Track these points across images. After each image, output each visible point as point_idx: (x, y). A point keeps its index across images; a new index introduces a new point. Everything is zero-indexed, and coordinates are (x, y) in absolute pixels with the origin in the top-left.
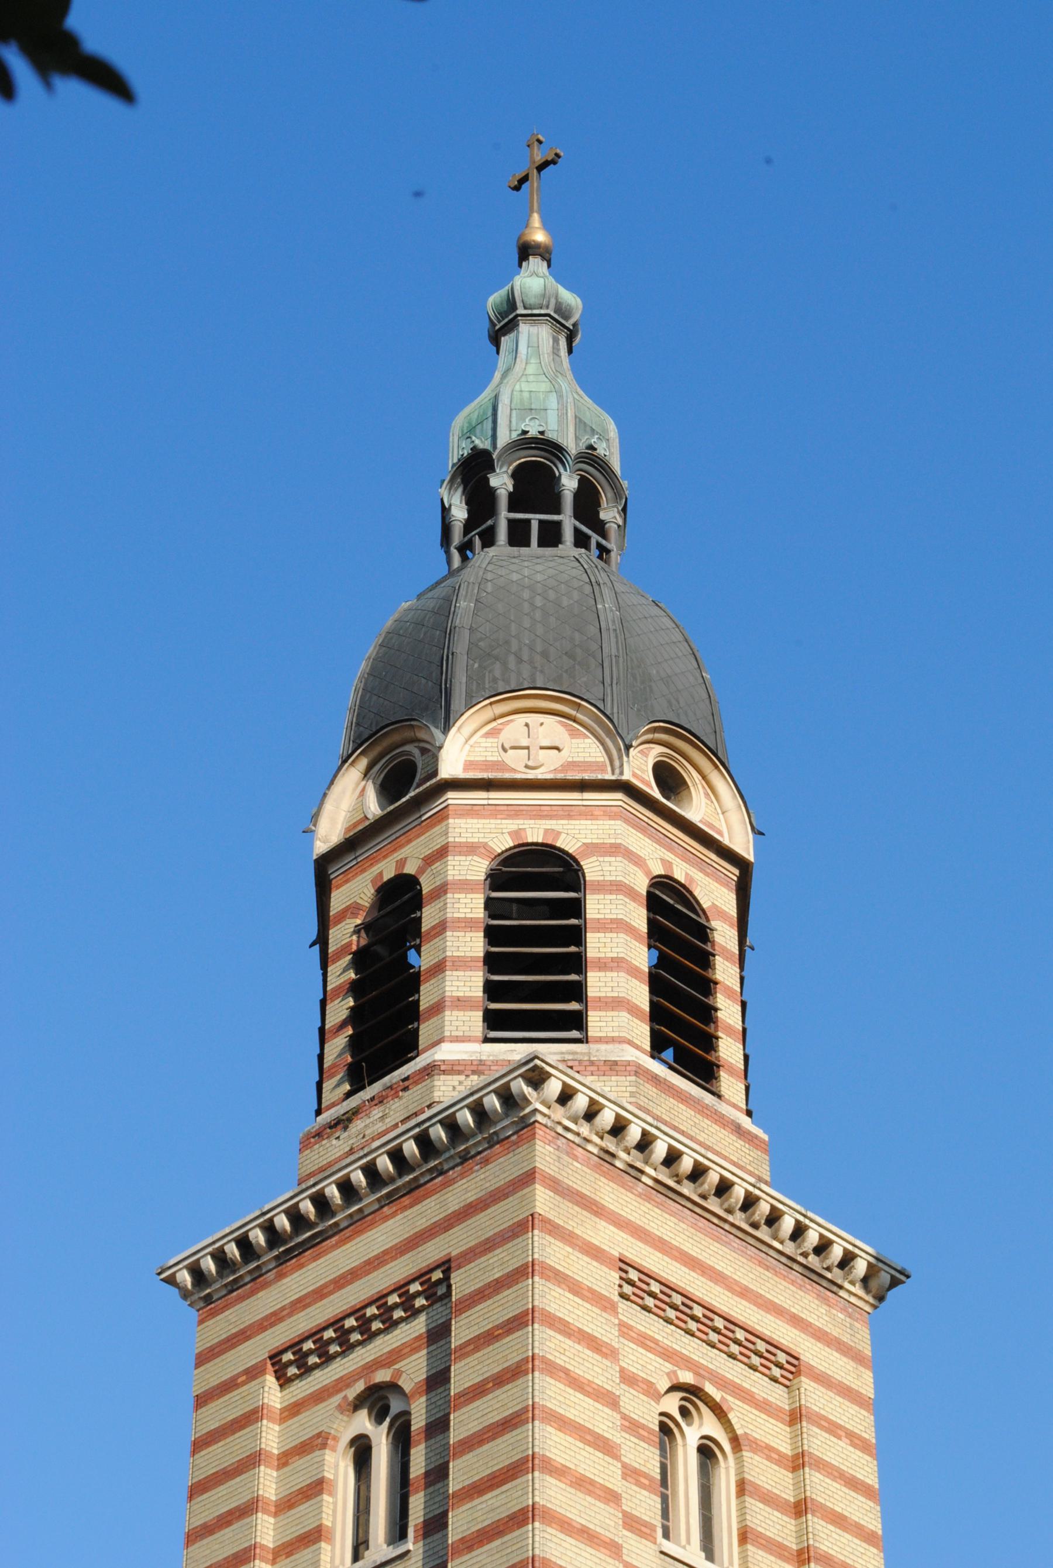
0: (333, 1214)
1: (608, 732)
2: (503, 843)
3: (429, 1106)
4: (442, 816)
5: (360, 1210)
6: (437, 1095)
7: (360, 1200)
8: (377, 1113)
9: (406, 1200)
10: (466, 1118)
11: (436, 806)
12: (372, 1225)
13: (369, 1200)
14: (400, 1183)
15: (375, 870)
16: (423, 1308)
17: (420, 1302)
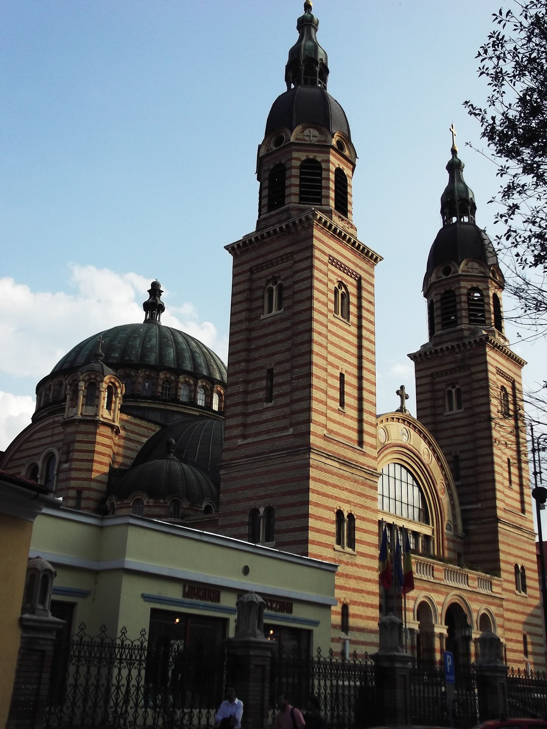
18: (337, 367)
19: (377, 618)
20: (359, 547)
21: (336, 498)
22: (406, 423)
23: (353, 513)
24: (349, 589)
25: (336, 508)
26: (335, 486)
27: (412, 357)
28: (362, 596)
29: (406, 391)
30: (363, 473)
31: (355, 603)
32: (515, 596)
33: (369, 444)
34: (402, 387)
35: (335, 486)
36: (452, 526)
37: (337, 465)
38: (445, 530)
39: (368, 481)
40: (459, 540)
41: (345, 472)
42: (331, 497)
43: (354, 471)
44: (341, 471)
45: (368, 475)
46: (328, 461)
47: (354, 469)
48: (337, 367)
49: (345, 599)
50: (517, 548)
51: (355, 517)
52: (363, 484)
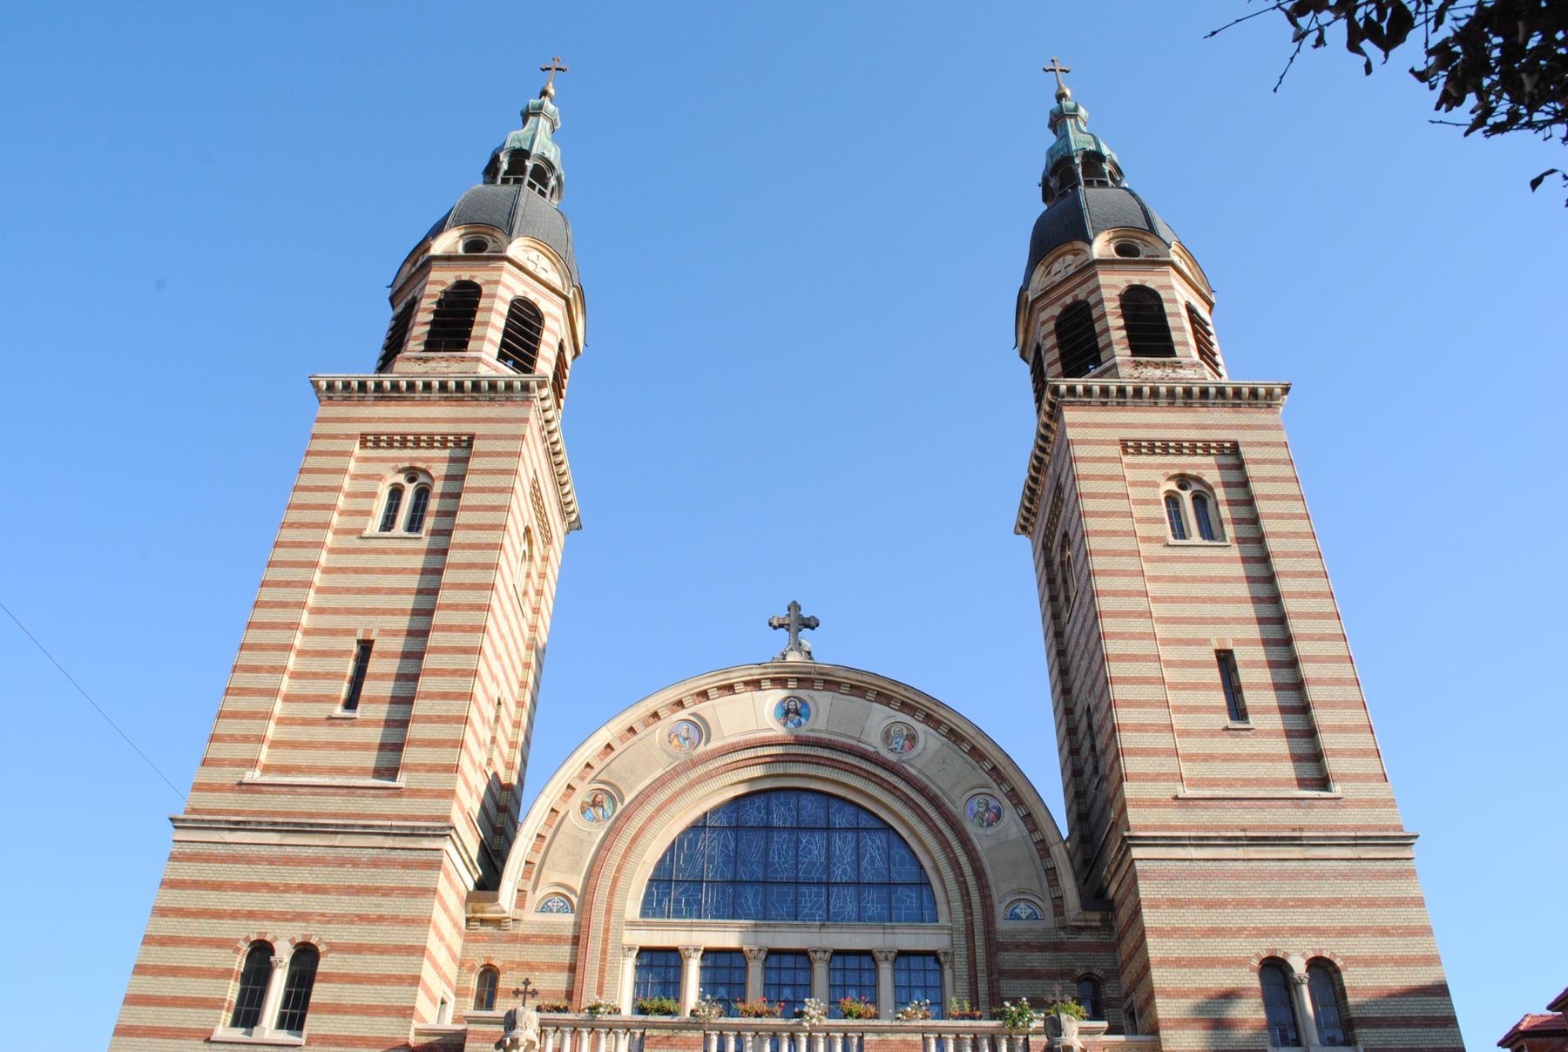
0: (414, 392)
1: (566, 277)
2: (520, 293)
3: (474, 373)
4: (500, 269)
5: (429, 397)
6: (479, 370)
7: (431, 393)
8: (444, 364)
9: (454, 403)
10: (485, 384)
11: (499, 264)
12: (433, 405)
13: (435, 395)
14: (455, 395)
15: (458, 273)
16: (451, 447)
17: (449, 444)
18: (350, 632)
20: (313, 1023)
21: (251, 915)
22: (792, 684)
23: (314, 941)
26: (250, 887)
27: (1020, 530)
29: (805, 613)
30: (380, 838)
33: (425, 765)
34: (795, 607)
35: (250, 887)
36: (1047, 906)
38: (1003, 924)
39: (400, 852)
40: (1085, 938)
42: (234, 915)
43: (338, 840)
47: (339, 836)
48: (350, 632)
50: (1269, 904)
51: (322, 948)
52: (375, 864)
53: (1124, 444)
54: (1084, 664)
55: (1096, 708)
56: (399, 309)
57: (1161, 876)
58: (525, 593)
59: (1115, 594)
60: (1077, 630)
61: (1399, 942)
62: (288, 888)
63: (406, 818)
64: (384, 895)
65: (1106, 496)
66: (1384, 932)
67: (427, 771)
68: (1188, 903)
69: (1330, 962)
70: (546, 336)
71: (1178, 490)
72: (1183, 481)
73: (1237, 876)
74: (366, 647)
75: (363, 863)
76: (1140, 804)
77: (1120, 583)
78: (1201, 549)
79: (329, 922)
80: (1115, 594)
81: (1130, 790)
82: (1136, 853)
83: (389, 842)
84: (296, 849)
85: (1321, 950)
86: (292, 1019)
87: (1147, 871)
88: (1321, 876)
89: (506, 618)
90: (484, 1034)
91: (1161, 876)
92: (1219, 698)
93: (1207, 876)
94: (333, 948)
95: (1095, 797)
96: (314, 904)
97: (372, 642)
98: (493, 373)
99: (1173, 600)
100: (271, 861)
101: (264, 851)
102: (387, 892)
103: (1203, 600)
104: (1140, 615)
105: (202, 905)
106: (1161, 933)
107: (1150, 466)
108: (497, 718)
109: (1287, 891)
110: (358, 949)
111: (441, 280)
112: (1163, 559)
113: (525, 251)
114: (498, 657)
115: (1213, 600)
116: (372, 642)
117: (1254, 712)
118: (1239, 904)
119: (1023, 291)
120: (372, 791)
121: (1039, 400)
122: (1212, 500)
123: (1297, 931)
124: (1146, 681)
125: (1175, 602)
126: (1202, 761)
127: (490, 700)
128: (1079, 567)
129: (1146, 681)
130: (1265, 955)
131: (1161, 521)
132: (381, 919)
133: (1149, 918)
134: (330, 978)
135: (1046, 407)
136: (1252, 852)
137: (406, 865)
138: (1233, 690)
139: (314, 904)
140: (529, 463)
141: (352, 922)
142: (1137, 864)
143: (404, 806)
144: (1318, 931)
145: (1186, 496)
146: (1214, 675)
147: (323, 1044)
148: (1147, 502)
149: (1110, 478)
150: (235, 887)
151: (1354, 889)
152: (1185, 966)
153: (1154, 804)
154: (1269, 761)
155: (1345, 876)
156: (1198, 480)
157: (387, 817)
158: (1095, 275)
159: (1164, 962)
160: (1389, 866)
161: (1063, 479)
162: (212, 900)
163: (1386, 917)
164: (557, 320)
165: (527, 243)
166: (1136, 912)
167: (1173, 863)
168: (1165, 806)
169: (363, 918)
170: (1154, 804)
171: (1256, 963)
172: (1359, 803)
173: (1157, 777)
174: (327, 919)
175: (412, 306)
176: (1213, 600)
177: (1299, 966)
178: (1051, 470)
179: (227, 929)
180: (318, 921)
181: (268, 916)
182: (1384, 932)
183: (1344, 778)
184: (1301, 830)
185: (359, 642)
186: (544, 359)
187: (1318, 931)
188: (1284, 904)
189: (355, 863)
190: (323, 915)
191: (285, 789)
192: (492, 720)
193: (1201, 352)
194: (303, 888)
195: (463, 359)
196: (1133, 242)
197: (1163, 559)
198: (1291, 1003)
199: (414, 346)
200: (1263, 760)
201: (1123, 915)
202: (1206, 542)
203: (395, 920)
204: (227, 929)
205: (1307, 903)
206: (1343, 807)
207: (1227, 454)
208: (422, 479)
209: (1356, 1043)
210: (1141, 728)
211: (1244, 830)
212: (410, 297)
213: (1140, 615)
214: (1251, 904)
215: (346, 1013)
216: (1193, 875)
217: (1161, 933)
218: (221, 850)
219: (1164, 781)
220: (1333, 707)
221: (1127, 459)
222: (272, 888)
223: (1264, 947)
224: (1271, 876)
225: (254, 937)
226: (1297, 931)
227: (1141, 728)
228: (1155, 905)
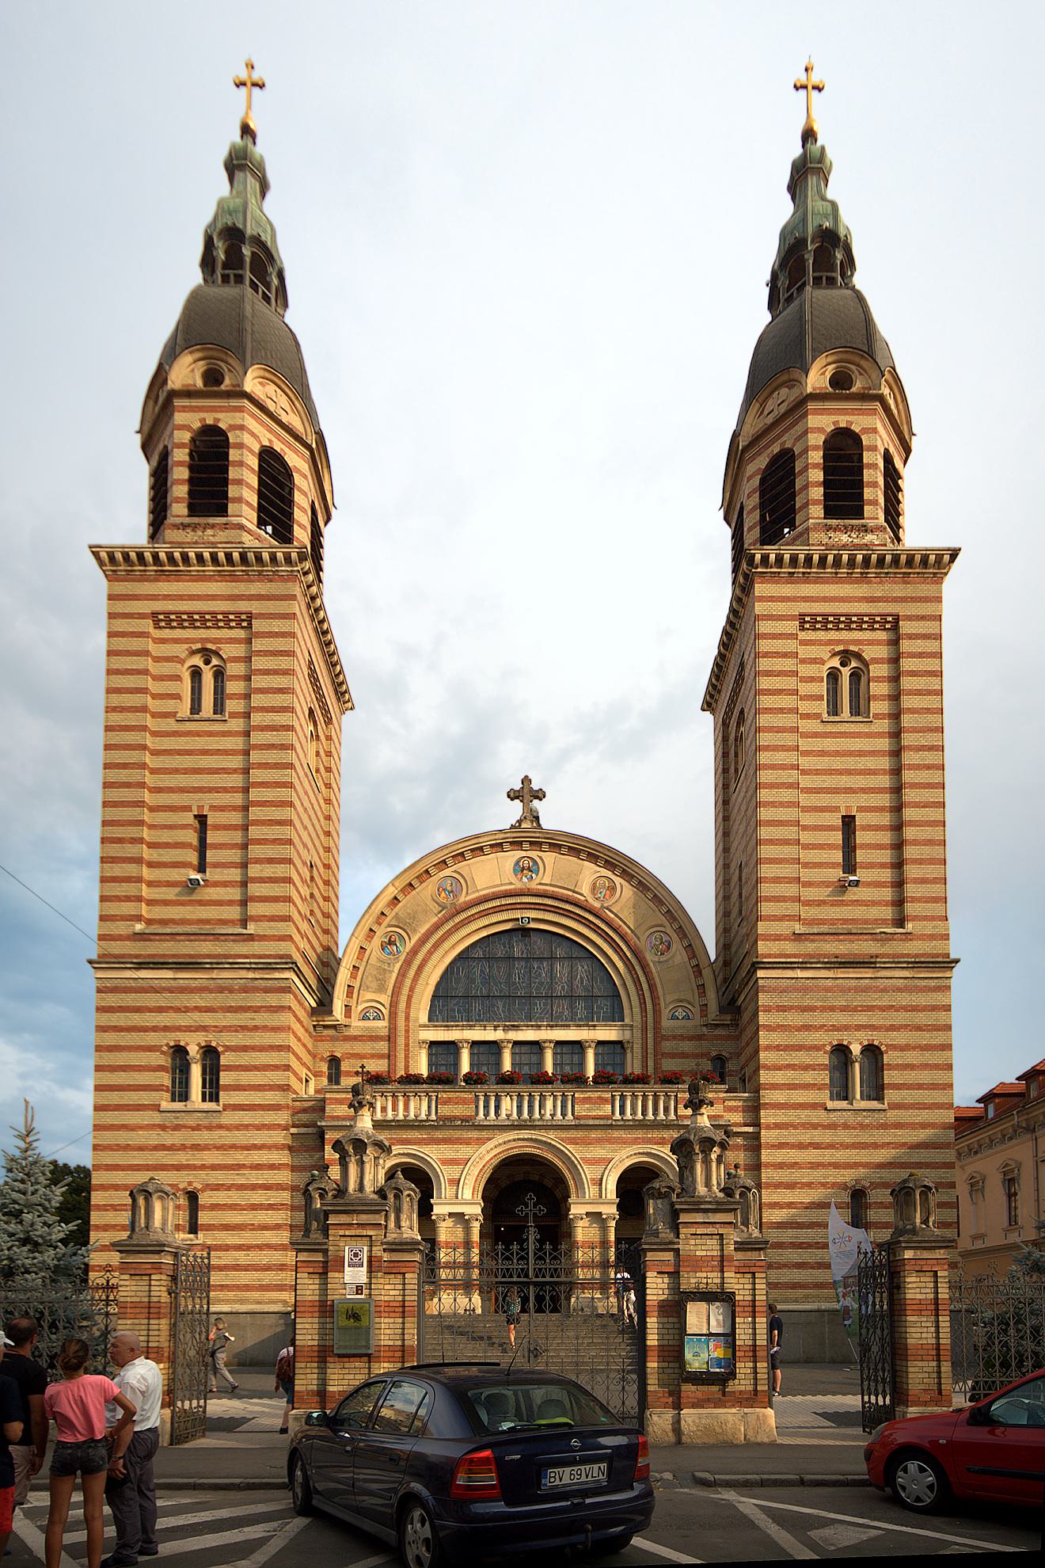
18: (188, 809)
19: (284, 1204)
21: (166, 1029)
23: (214, 1044)
24: (203, 1167)
25: (167, 1045)
26: (160, 1010)
28: (238, 1174)
30: (244, 972)
31: (209, 1187)
32: (822, 1113)
33: (266, 916)
37: (169, 974)
41: (191, 982)
42: (155, 1029)
44: (181, 981)
45: (261, 971)
46: (143, 974)
47: (216, 971)
48: (188, 809)
49: (190, 1183)
50: (844, 1009)
51: (220, 1049)
52: (245, 990)
53: (801, 617)
54: (741, 830)
55: (746, 865)
56: (155, 462)
57: (775, 990)
58: (317, 771)
59: (773, 767)
60: (740, 800)
61: (927, 1035)
62: (187, 1010)
63: (260, 957)
64: (255, 1012)
65: (780, 673)
66: (919, 1028)
67: (268, 921)
68: (790, 1008)
69: (877, 1047)
70: (298, 497)
71: (839, 667)
72: (846, 656)
73: (827, 990)
74: (202, 819)
75: (236, 990)
76: (768, 938)
77: (780, 757)
78: (847, 725)
79: (221, 1032)
80: (773, 767)
81: (762, 928)
82: (760, 974)
83: (251, 975)
84: (187, 982)
85: (873, 1040)
86: (212, 1091)
87: (765, 986)
88: (884, 990)
89: (306, 793)
90: (336, 1099)
91: (775, 990)
92: (838, 856)
93: (806, 990)
94: (228, 1048)
95: (737, 932)
96: (207, 1019)
97: (206, 816)
98: (257, 544)
99: (817, 772)
100: (171, 990)
101: (164, 984)
102: (256, 1010)
103: (840, 772)
104: (790, 786)
105: (130, 1023)
106: (770, 1028)
107: (819, 643)
108: (312, 878)
109: (859, 1000)
110: (245, 1049)
111: (187, 420)
112: (816, 735)
113: (261, 383)
114: (305, 828)
115: (848, 772)
116: (206, 816)
117: (860, 868)
118: (824, 1009)
119: (735, 436)
120: (231, 937)
121: (735, 570)
122: (866, 676)
123: (859, 1028)
124: (786, 842)
125: (819, 774)
126: (817, 905)
127: (304, 863)
128: (748, 742)
129: (786, 842)
130: (835, 1043)
131: (820, 698)
132: (256, 1028)
133: (763, 1018)
134: (229, 1068)
135: (741, 579)
136: (840, 973)
137: (267, 990)
138: (849, 848)
139: (207, 1019)
140: (302, 643)
141: (237, 1031)
142: (760, 982)
143: (256, 948)
144: (873, 1028)
145: (846, 672)
146: (837, 837)
147: (233, 1110)
148: (812, 679)
149: (785, 655)
150: (150, 1010)
151: (905, 999)
152: (781, 1050)
153: (778, 938)
154: (865, 906)
155: (899, 990)
156: (858, 656)
157: (246, 957)
158: (805, 415)
159: (768, 1048)
160: (932, 983)
161: (746, 657)
162: (136, 1019)
163: (922, 1018)
164: (305, 477)
165: (262, 373)
166: (756, 1015)
167: (784, 981)
168: (785, 940)
169: (244, 1028)
170: (778, 938)
171: (828, 1048)
172: (922, 937)
173: (781, 918)
174: (221, 1029)
175: (165, 455)
176: (848, 772)
177: (856, 1049)
178: (737, 647)
179: (152, 1039)
180: (214, 1031)
181: (179, 1029)
182: (919, 1028)
183: (915, 918)
184: (877, 957)
185: (195, 816)
186: (300, 525)
187: (873, 1028)
188: (855, 1009)
189: (231, 990)
190: (216, 1027)
191: (168, 937)
192: (308, 879)
193: (887, 512)
194: (198, 1009)
195: (226, 526)
196: (849, 369)
197: (816, 735)
198: (847, 1073)
199: (178, 510)
200: (860, 905)
201: (746, 1016)
202: (853, 719)
203: (265, 1028)
204: (152, 1039)
205: (870, 1008)
206: (911, 940)
207: (888, 629)
208: (215, 661)
209: (883, 1099)
210: (777, 880)
211: (837, 957)
212: (161, 447)
213: (790, 786)
214: (832, 1009)
215: (245, 1090)
216: (797, 990)
217: (770, 1028)
218: (133, 984)
219: (788, 921)
220: (921, 864)
221: (802, 635)
222: (177, 1010)
223: (835, 1038)
224: (850, 990)
225: (172, 1044)
226: (859, 1028)
227: (777, 880)
228: (768, 1010)
